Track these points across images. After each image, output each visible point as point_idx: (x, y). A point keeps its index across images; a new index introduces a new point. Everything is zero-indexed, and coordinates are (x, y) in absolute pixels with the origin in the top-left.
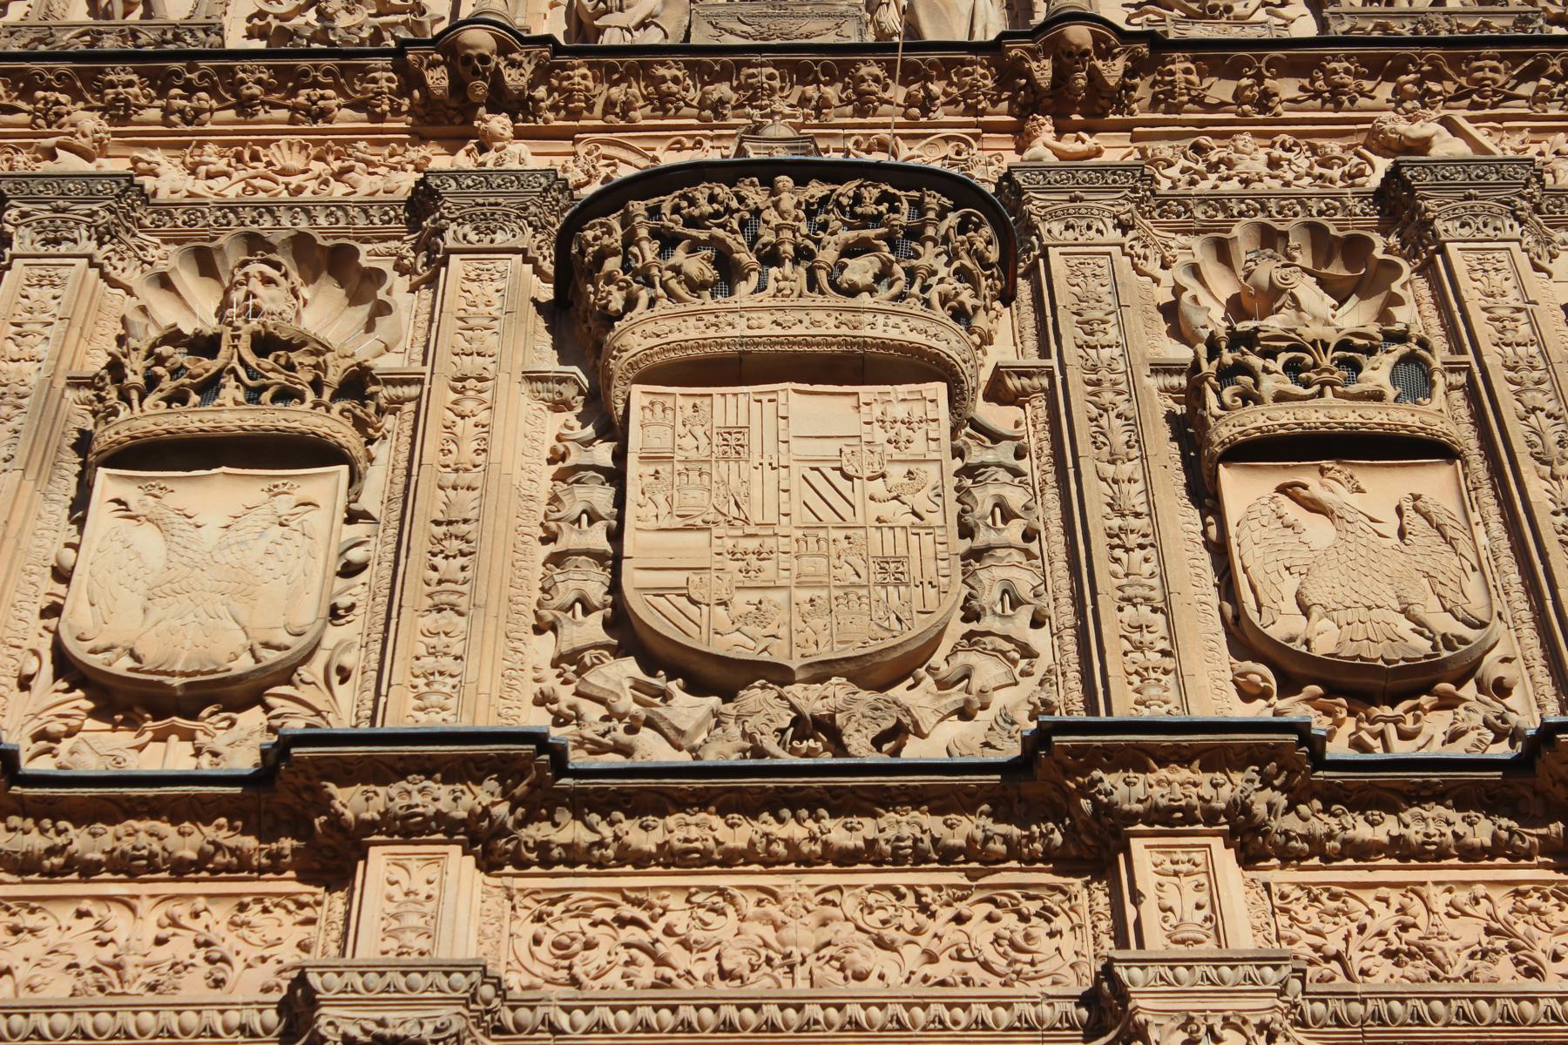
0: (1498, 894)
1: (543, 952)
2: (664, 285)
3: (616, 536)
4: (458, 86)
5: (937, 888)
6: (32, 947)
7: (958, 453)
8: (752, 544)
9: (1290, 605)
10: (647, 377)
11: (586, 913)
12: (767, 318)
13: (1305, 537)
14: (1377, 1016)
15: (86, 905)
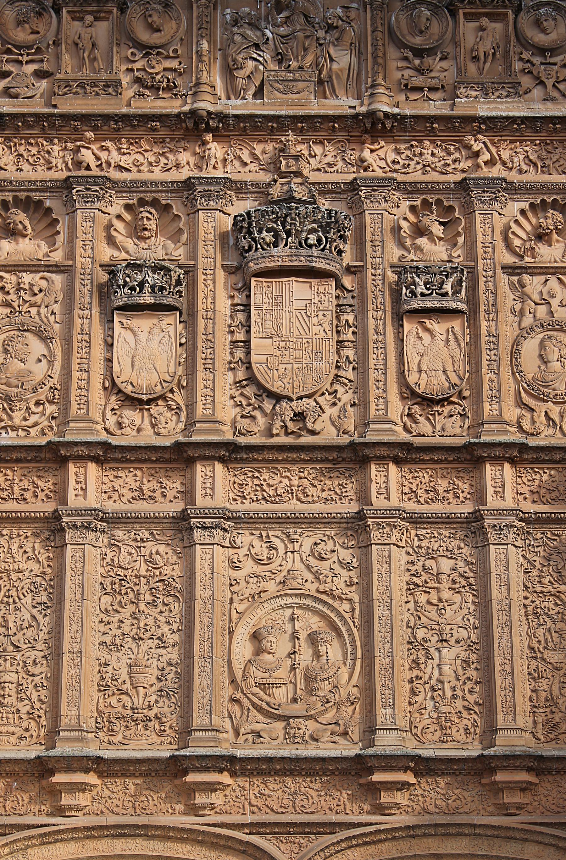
0: (453, 471)
1: (236, 486)
2: (260, 244)
3: (248, 332)
4: (196, 124)
5: (326, 468)
6: (120, 481)
7: (337, 297)
8: (283, 344)
9: (415, 369)
10: (256, 275)
11: (246, 474)
12: (287, 259)
13: (424, 342)
14: (420, 517)
15: (132, 470)
